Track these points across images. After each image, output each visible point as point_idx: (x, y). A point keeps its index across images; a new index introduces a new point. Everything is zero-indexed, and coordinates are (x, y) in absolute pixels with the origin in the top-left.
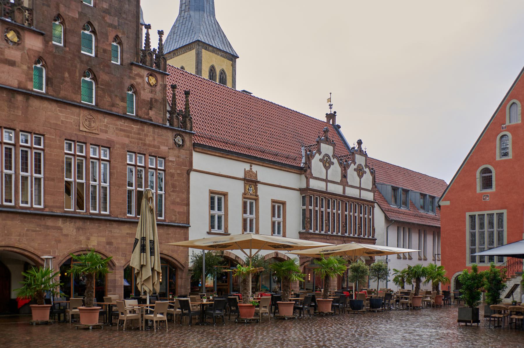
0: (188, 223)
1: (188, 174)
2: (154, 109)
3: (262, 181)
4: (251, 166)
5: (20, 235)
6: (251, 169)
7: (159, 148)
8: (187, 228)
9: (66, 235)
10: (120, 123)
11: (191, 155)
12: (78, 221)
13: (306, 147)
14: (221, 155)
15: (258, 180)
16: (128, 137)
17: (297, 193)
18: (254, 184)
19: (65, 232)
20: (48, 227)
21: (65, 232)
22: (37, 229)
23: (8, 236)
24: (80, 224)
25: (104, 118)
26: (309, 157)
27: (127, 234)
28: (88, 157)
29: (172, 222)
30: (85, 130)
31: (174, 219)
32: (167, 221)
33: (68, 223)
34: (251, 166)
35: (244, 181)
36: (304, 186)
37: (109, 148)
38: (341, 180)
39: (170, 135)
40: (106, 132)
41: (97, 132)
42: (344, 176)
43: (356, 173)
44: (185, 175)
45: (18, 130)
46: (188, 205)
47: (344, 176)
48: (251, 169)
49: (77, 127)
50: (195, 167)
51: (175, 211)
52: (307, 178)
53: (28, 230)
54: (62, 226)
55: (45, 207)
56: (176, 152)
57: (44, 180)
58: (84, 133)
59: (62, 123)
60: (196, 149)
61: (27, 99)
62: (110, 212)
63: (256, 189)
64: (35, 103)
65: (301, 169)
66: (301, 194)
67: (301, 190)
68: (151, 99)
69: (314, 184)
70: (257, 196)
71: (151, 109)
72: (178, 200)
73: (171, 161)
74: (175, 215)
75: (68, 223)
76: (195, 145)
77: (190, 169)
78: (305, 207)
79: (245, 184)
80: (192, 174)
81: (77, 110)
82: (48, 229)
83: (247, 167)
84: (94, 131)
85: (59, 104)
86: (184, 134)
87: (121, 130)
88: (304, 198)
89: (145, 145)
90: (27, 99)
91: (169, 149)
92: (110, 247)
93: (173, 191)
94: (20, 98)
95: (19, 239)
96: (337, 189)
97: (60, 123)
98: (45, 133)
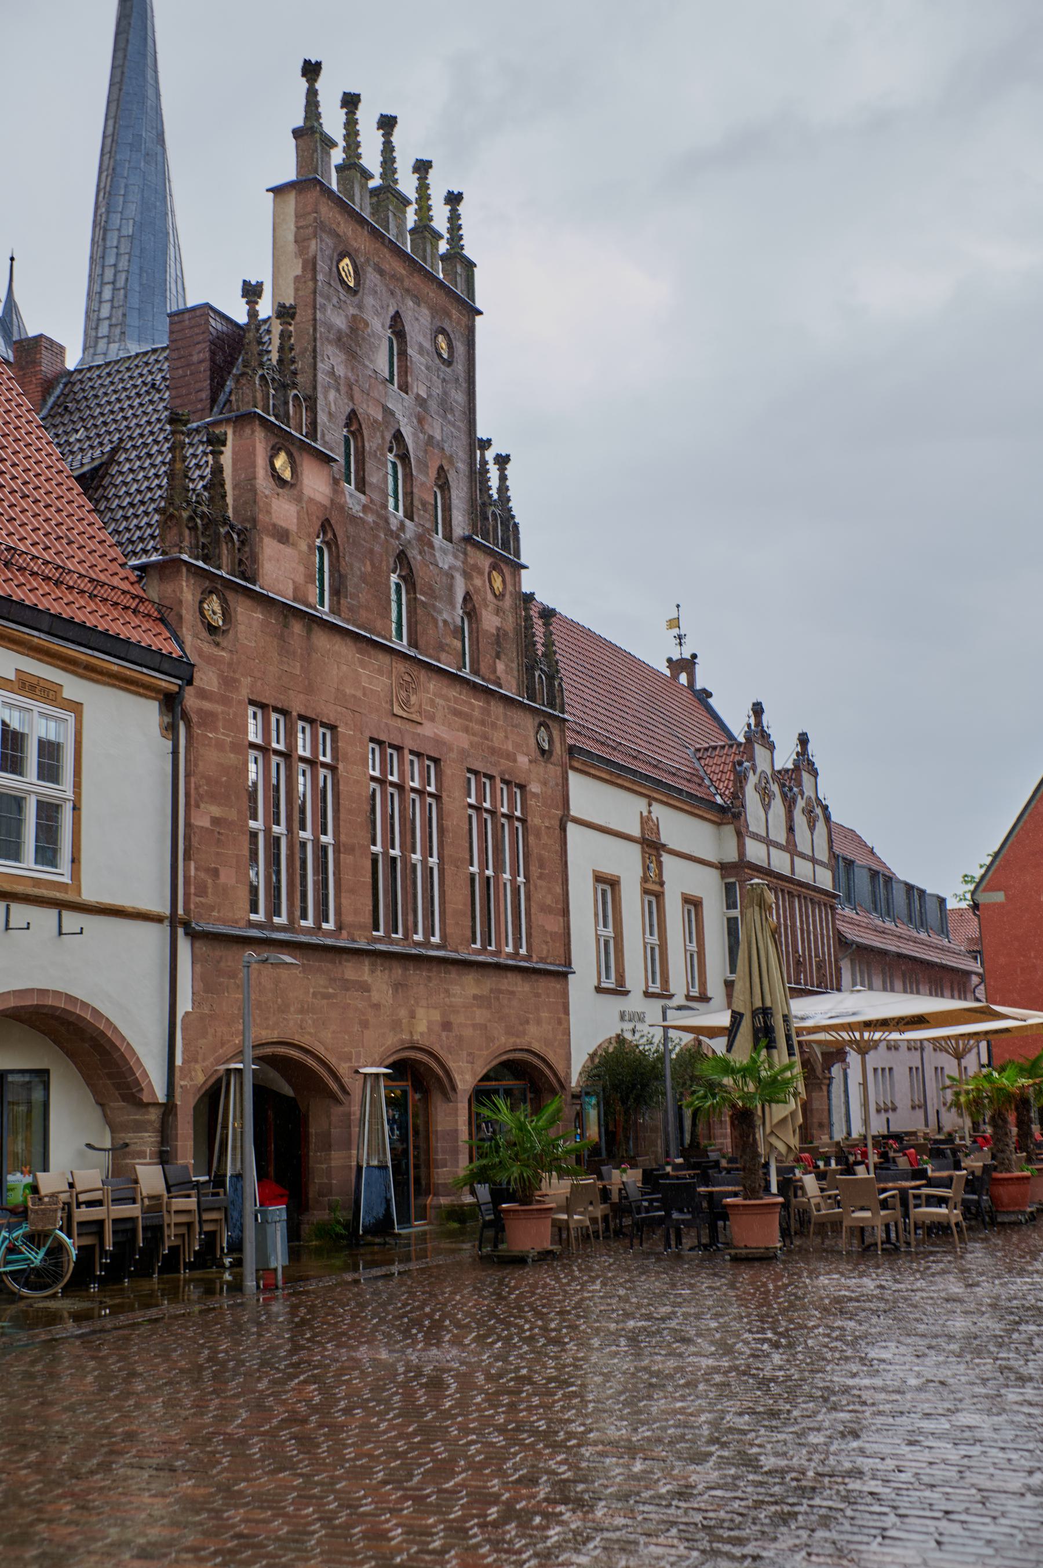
0: (568, 963)
1: (563, 829)
2: (503, 656)
3: (671, 846)
4: (650, 805)
5: (302, 1011)
6: (650, 812)
7: (515, 761)
8: (564, 975)
9: (377, 1006)
10: (453, 692)
11: (565, 779)
12: (395, 964)
13: (698, 750)
14: (607, 777)
15: (663, 840)
16: (466, 730)
17: (714, 875)
18: (654, 852)
19: (375, 997)
20: (347, 985)
21: (375, 997)
22: (331, 990)
23: (283, 1012)
24: (398, 971)
25: (430, 679)
26: (740, 780)
27: (475, 997)
28: (407, 788)
29: (542, 960)
30: (401, 713)
31: (544, 954)
32: (535, 959)
33: (379, 973)
34: (650, 805)
35: (641, 844)
36: (732, 856)
37: (436, 761)
38: (787, 841)
39: (529, 723)
40: (432, 718)
41: (419, 720)
42: (791, 829)
43: (804, 819)
44: (557, 831)
45: (294, 714)
46: (566, 912)
47: (791, 829)
48: (650, 812)
49: (388, 706)
50: (574, 812)
51: (546, 931)
52: (740, 835)
53: (314, 994)
54: (370, 981)
55: (340, 927)
56: (540, 769)
57: (337, 851)
58: (399, 720)
59: (364, 695)
60: (576, 764)
61: (309, 631)
62: (443, 937)
63: (660, 864)
64: (322, 640)
65: (722, 810)
66: (723, 877)
67: (724, 868)
68: (498, 629)
69: (755, 852)
70: (662, 884)
71: (498, 656)
72: (549, 901)
73: (535, 795)
74: (547, 943)
75: (379, 973)
76: (572, 750)
77: (565, 819)
78: (735, 913)
79: (643, 852)
80: (571, 827)
81: (384, 659)
82: (347, 989)
83: (640, 805)
84: (414, 717)
85: (359, 645)
86: (550, 723)
87: (457, 713)
88: (729, 889)
89: (493, 751)
90: (309, 631)
91: (530, 761)
92: (447, 1038)
93: (541, 877)
94: (297, 627)
95: (302, 1020)
96: (780, 862)
97: (359, 694)
98: (338, 723)
